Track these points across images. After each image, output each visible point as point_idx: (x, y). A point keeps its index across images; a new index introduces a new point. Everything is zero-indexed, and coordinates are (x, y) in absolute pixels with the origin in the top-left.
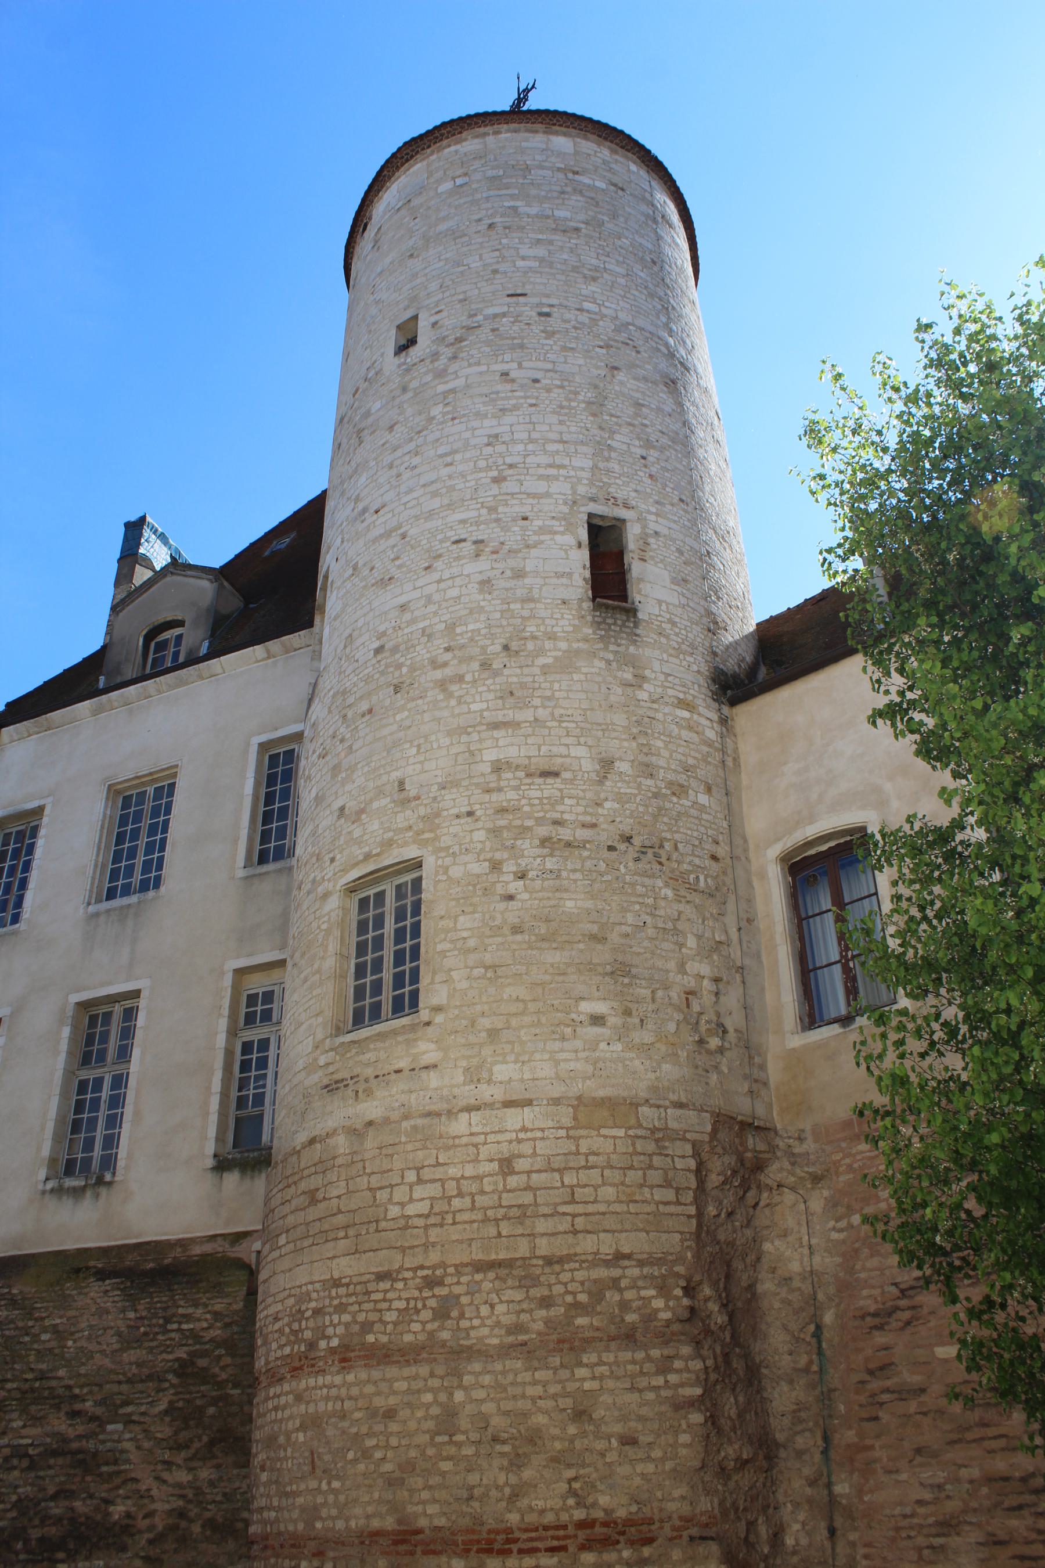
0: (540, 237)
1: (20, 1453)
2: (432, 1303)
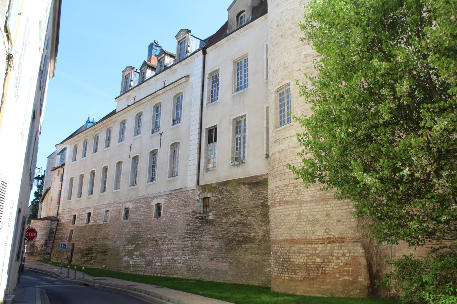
1: (232, 223)
2: (296, 191)
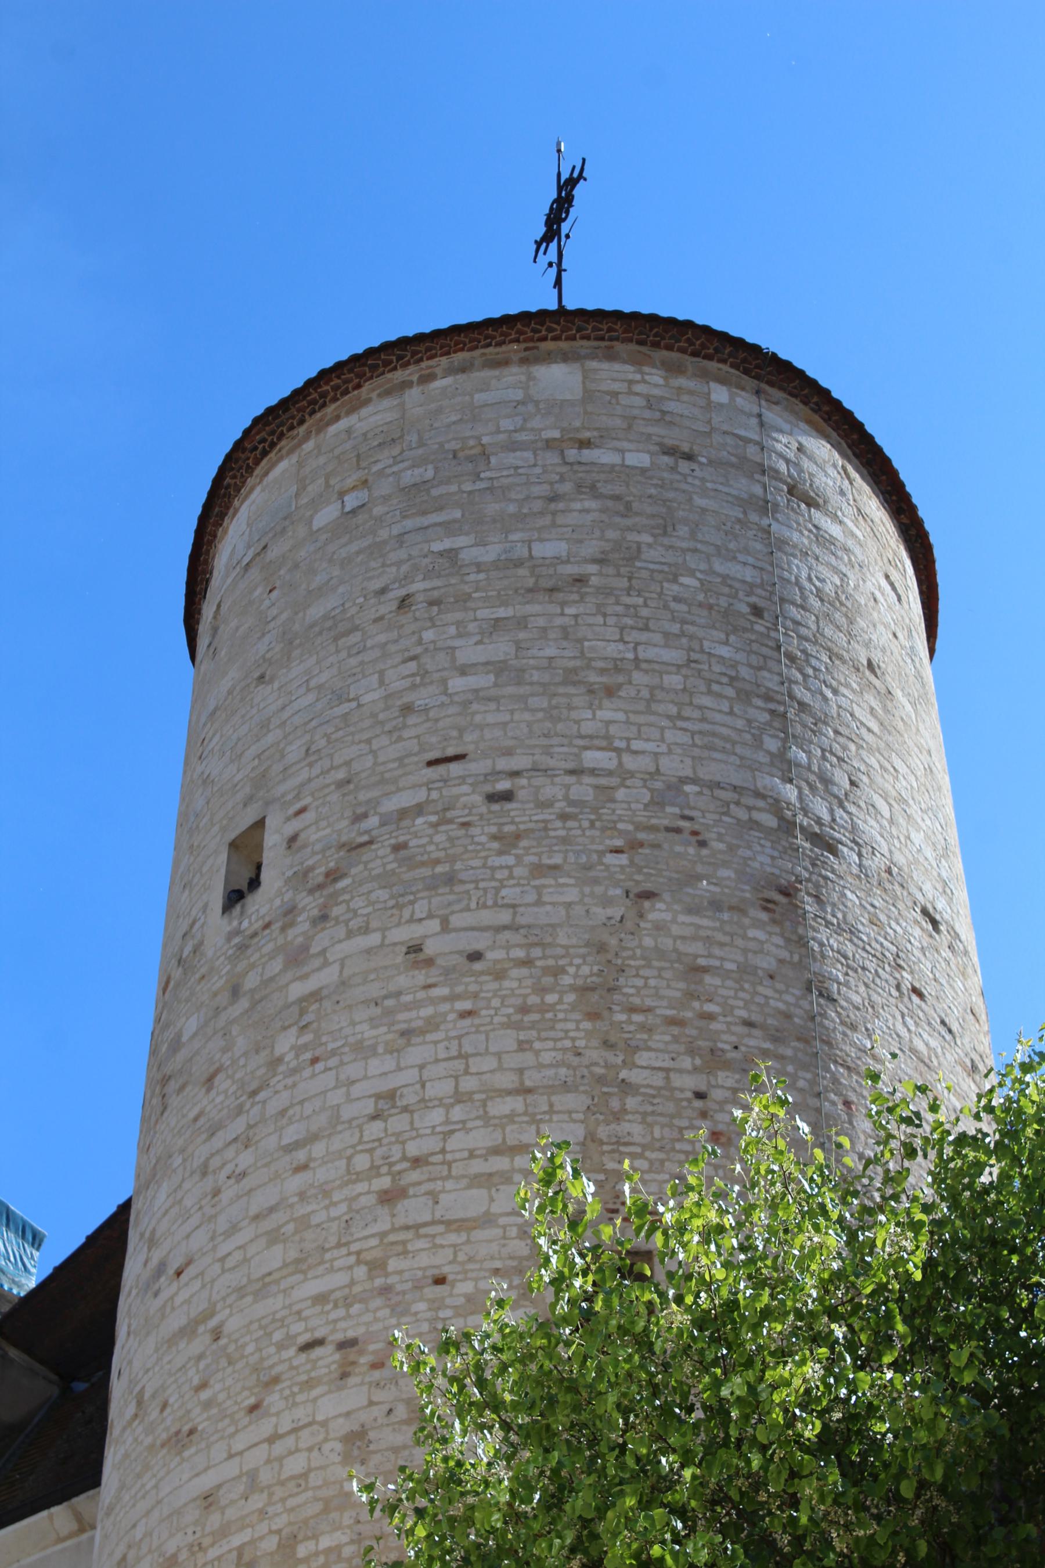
0: (501, 612)
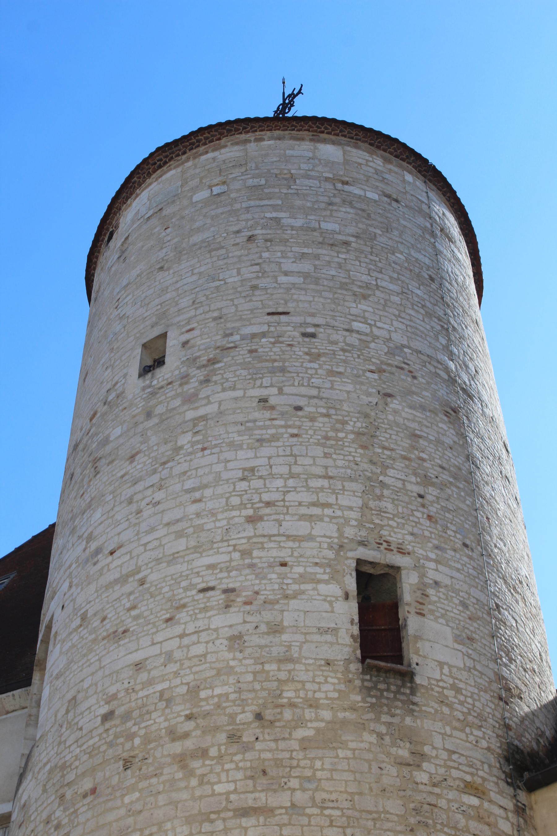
0: (305, 250)
